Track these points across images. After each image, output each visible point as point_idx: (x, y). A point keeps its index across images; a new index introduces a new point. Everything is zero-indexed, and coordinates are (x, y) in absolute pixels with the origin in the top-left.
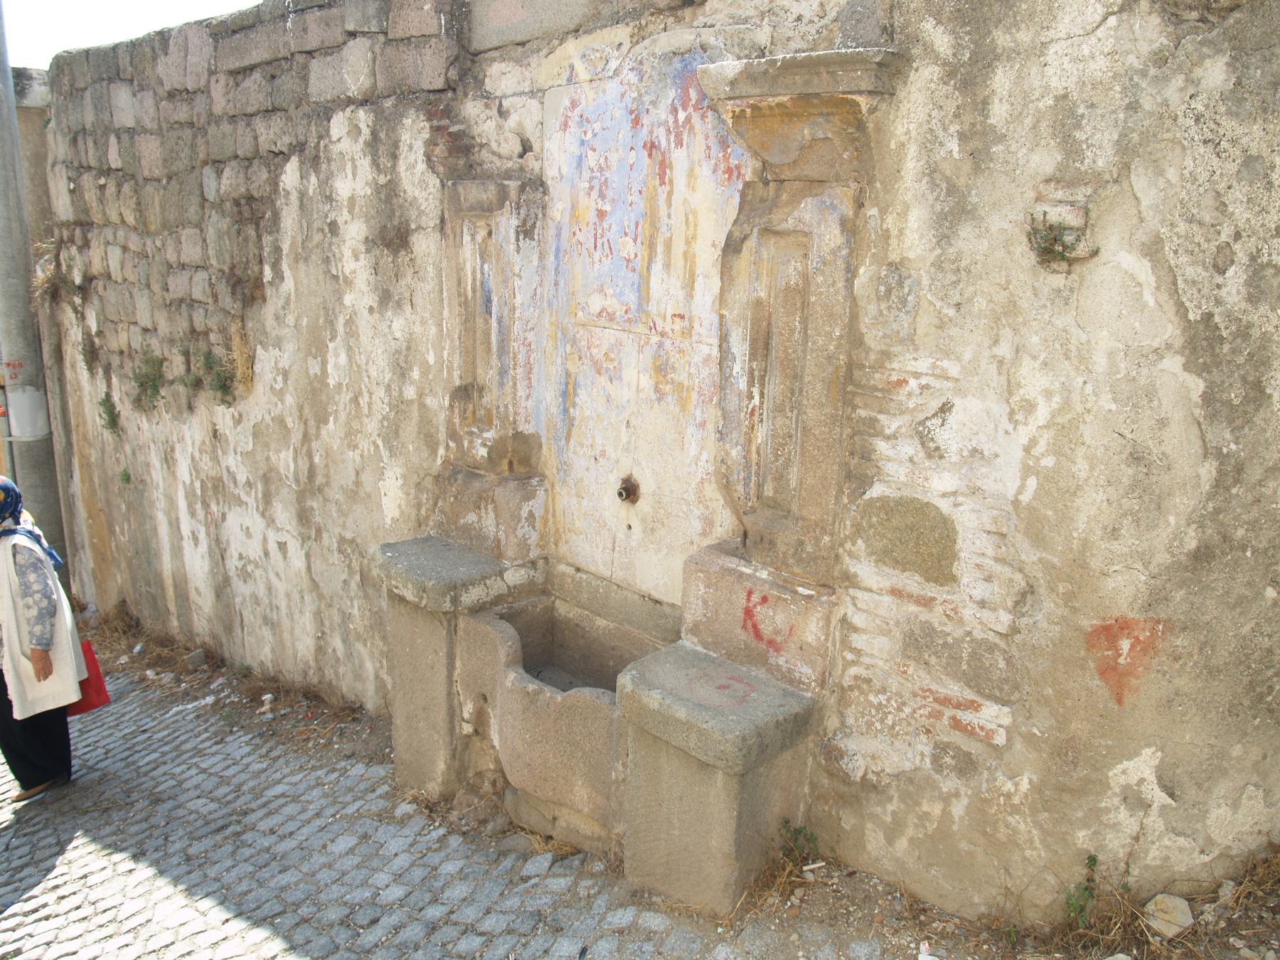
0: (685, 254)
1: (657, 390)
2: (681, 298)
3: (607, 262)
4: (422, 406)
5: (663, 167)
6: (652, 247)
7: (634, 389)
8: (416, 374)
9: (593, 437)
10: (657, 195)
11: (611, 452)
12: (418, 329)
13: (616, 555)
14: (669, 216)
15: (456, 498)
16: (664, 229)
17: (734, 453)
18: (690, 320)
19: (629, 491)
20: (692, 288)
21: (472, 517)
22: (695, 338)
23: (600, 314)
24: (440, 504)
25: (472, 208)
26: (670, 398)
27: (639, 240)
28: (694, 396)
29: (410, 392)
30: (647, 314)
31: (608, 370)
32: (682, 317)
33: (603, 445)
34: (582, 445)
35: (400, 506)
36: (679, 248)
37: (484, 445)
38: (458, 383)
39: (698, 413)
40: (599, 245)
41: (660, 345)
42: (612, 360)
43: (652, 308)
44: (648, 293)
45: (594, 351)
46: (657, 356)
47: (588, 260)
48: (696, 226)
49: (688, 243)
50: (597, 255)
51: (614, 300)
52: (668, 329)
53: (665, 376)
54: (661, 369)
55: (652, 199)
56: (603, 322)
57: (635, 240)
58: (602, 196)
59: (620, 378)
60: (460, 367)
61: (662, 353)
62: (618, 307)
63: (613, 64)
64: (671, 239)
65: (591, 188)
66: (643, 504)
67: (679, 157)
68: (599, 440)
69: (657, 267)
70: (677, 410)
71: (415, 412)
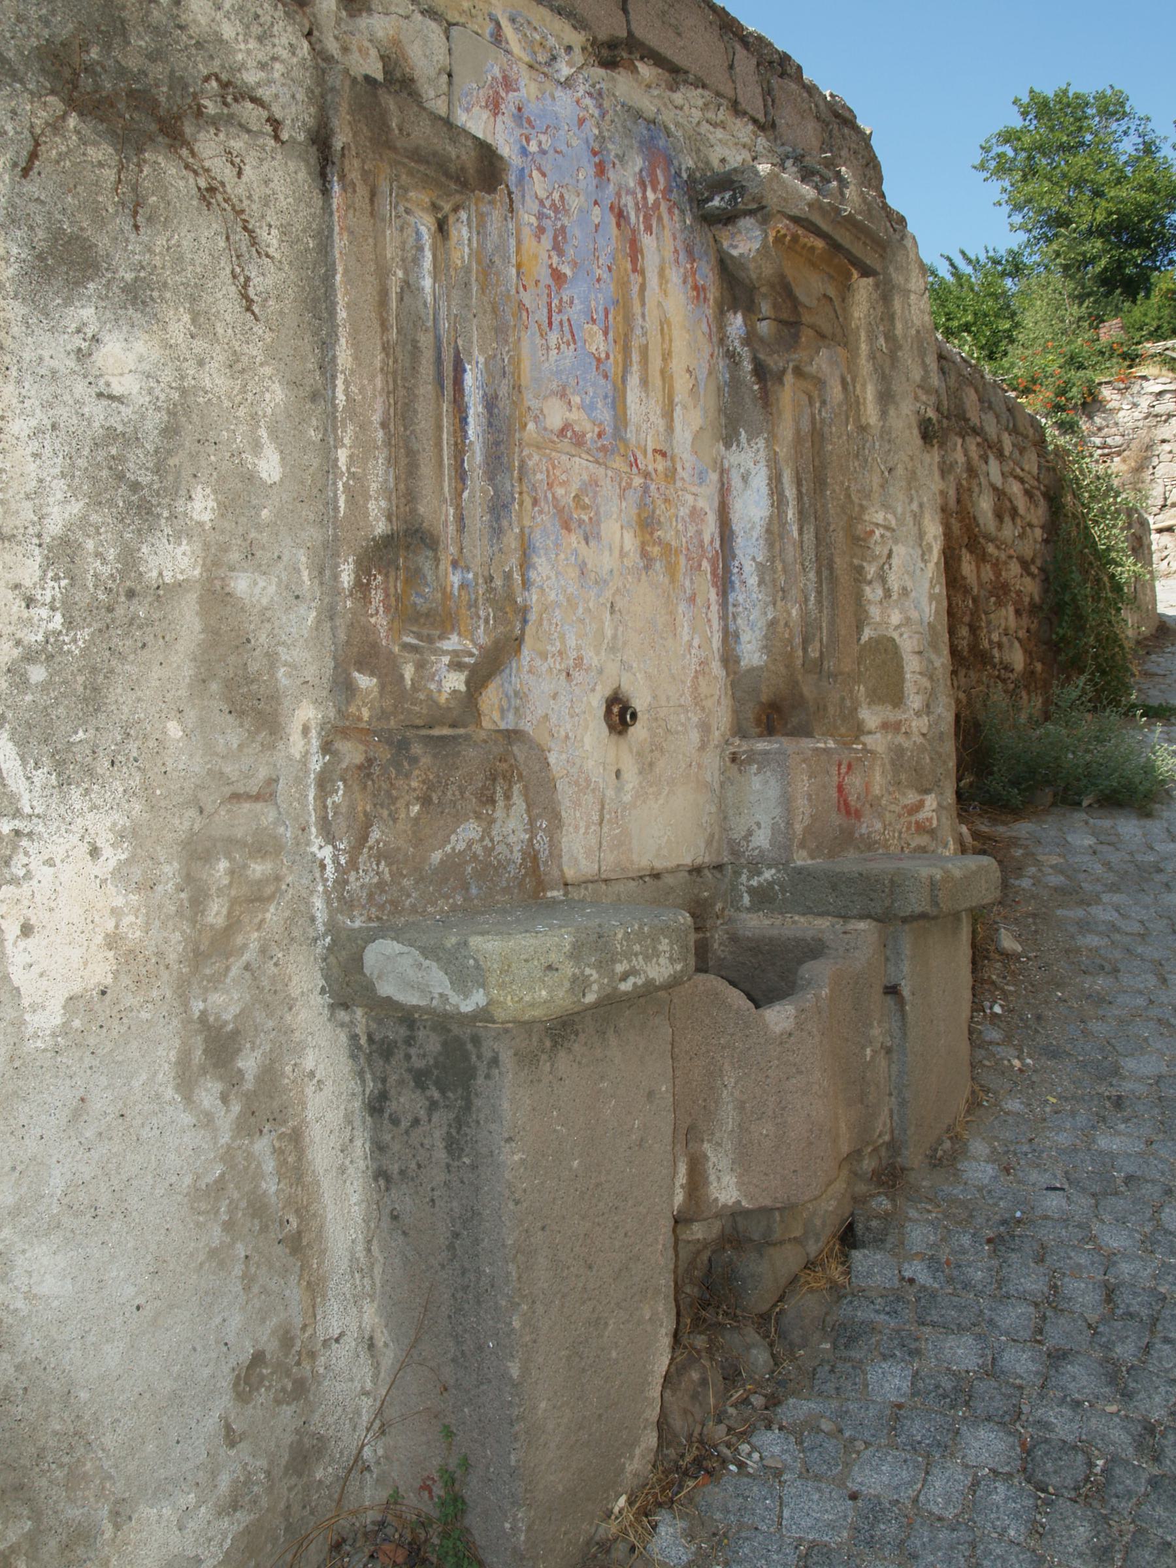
0: (663, 372)
1: (644, 554)
2: (661, 429)
3: (569, 352)
4: (216, 596)
5: (635, 251)
6: (626, 350)
7: (616, 552)
8: (202, 506)
9: (562, 637)
10: (629, 282)
11: (592, 658)
12: (215, 380)
13: (605, 829)
14: (643, 316)
15: (426, 801)
16: (638, 332)
17: (794, 612)
18: (673, 459)
19: (620, 714)
20: (672, 420)
21: (468, 832)
22: (679, 484)
23: (562, 432)
24: (375, 834)
25: (416, 155)
26: (658, 564)
27: (611, 335)
28: (682, 560)
29: (172, 560)
30: (624, 441)
31: (581, 522)
32: (664, 455)
33: (579, 648)
34: (544, 656)
35: (112, 941)
36: (656, 363)
37: (457, 666)
38: (381, 527)
39: (687, 583)
40: (555, 324)
41: (646, 489)
42: (585, 508)
43: (631, 435)
44: (625, 414)
45: (560, 491)
46: (642, 506)
47: (538, 341)
48: (671, 340)
49: (664, 360)
50: (553, 338)
51: (583, 416)
52: (650, 468)
53: (652, 534)
54: (646, 524)
55: (623, 285)
56: (565, 444)
57: (606, 333)
58: (557, 248)
59: (598, 537)
60: (386, 492)
61: (649, 501)
62: (588, 426)
63: (565, 71)
64: (646, 346)
65: (541, 230)
66: (638, 732)
67: (648, 242)
68: (572, 642)
69: (634, 380)
70: (667, 581)
71: (188, 621)
